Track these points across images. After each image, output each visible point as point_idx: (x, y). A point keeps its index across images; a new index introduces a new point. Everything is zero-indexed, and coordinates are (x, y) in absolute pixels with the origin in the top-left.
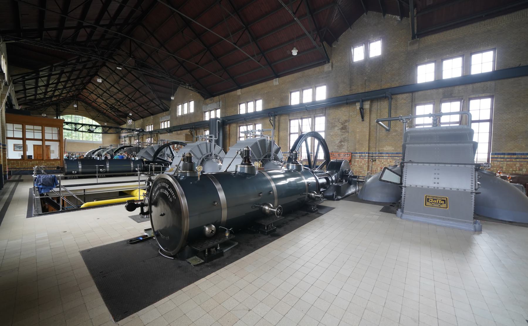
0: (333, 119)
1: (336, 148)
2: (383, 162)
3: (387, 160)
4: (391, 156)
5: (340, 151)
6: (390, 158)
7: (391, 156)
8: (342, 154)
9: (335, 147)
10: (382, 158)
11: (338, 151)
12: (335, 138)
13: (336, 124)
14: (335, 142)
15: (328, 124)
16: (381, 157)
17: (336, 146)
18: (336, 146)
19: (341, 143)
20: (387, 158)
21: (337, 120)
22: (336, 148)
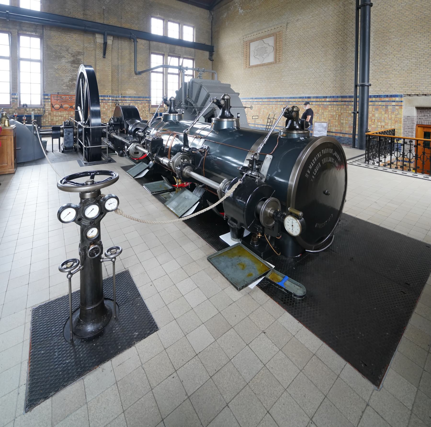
0: (59, 46)
1: (65, 88)
4: (133, 100)
5: (72, 92)
7: (133, 100)
9: (62, 87)
11: (68, 93)
12: (63, 75)
13: (63, 54)
14: (62, 80)
15: (49, 52)
17: (65, 85)
18: (65, 85)
19: (73, 81)
21: (65, 49)
22: (65, 88)
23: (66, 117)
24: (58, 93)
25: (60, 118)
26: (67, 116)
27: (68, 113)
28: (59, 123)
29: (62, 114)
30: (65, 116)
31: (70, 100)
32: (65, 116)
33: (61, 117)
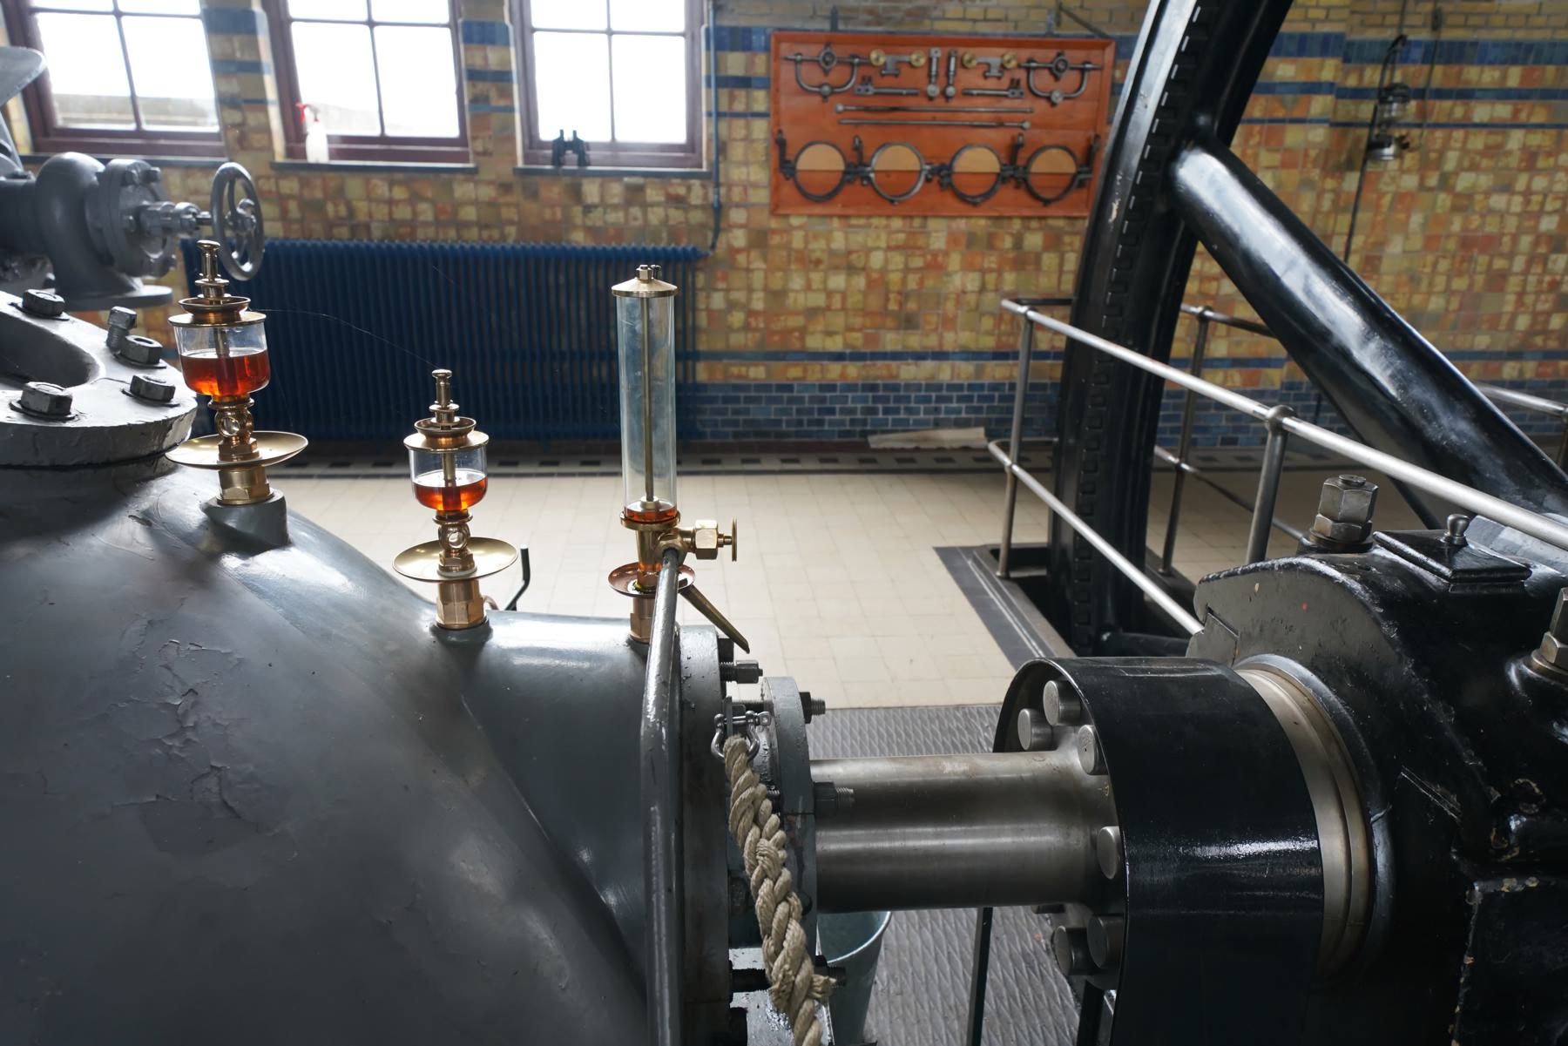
2: (1460, 169)
3: (1495, 139)
6: (1540, 116)
8: (993, 57)
10: (1459, 111)
16: (1442, 109)
20: (1503, 111)
23: (884, 271)
24: (834, 18)
25: (838, 281)
26: (898, 260)
27: (911, 234)
28: (829, 334)
29: (858, 239)
30: (877, 260)
31: (933, 89)
32: (877, 260)
33: (851, 269)
